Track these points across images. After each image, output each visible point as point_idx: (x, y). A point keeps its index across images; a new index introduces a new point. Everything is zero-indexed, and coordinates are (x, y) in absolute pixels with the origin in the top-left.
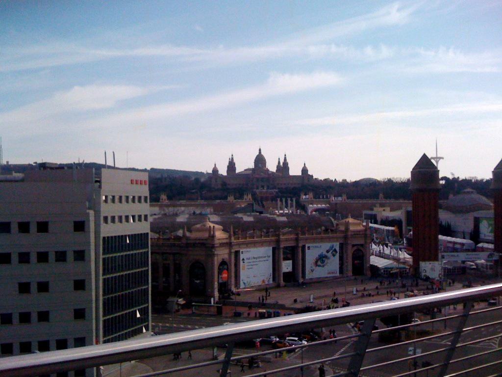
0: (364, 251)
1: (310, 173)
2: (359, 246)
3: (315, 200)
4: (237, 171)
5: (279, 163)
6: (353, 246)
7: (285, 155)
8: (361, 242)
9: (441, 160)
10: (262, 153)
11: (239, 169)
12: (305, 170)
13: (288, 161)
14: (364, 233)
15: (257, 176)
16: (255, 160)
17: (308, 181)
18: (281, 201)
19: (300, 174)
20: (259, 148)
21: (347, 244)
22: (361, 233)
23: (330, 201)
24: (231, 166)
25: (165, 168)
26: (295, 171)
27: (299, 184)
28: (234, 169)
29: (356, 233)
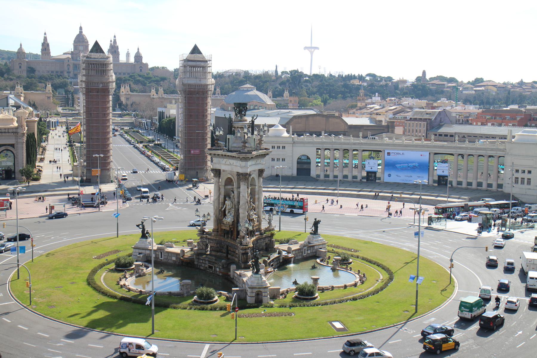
0: (15, 152)
1: (144, 61)
2: (6, 147)
4: (52, 54)
5: (111, 44)
7: (115, 37)
8: (12, 142)
9: (316, 50)
10: (84, 33)
11: (56, 51)
12: (138, 57)
13: (118, 44)
14: (14, 131)
16: (74, 41)
17: (141, 70)
19: (132, 60)
20: (80, 26)
22: (10, 131)
23: (150, 95)
24: (45, 47)
27: (128, 74)
28: (49, 53)
29: (4, 131)
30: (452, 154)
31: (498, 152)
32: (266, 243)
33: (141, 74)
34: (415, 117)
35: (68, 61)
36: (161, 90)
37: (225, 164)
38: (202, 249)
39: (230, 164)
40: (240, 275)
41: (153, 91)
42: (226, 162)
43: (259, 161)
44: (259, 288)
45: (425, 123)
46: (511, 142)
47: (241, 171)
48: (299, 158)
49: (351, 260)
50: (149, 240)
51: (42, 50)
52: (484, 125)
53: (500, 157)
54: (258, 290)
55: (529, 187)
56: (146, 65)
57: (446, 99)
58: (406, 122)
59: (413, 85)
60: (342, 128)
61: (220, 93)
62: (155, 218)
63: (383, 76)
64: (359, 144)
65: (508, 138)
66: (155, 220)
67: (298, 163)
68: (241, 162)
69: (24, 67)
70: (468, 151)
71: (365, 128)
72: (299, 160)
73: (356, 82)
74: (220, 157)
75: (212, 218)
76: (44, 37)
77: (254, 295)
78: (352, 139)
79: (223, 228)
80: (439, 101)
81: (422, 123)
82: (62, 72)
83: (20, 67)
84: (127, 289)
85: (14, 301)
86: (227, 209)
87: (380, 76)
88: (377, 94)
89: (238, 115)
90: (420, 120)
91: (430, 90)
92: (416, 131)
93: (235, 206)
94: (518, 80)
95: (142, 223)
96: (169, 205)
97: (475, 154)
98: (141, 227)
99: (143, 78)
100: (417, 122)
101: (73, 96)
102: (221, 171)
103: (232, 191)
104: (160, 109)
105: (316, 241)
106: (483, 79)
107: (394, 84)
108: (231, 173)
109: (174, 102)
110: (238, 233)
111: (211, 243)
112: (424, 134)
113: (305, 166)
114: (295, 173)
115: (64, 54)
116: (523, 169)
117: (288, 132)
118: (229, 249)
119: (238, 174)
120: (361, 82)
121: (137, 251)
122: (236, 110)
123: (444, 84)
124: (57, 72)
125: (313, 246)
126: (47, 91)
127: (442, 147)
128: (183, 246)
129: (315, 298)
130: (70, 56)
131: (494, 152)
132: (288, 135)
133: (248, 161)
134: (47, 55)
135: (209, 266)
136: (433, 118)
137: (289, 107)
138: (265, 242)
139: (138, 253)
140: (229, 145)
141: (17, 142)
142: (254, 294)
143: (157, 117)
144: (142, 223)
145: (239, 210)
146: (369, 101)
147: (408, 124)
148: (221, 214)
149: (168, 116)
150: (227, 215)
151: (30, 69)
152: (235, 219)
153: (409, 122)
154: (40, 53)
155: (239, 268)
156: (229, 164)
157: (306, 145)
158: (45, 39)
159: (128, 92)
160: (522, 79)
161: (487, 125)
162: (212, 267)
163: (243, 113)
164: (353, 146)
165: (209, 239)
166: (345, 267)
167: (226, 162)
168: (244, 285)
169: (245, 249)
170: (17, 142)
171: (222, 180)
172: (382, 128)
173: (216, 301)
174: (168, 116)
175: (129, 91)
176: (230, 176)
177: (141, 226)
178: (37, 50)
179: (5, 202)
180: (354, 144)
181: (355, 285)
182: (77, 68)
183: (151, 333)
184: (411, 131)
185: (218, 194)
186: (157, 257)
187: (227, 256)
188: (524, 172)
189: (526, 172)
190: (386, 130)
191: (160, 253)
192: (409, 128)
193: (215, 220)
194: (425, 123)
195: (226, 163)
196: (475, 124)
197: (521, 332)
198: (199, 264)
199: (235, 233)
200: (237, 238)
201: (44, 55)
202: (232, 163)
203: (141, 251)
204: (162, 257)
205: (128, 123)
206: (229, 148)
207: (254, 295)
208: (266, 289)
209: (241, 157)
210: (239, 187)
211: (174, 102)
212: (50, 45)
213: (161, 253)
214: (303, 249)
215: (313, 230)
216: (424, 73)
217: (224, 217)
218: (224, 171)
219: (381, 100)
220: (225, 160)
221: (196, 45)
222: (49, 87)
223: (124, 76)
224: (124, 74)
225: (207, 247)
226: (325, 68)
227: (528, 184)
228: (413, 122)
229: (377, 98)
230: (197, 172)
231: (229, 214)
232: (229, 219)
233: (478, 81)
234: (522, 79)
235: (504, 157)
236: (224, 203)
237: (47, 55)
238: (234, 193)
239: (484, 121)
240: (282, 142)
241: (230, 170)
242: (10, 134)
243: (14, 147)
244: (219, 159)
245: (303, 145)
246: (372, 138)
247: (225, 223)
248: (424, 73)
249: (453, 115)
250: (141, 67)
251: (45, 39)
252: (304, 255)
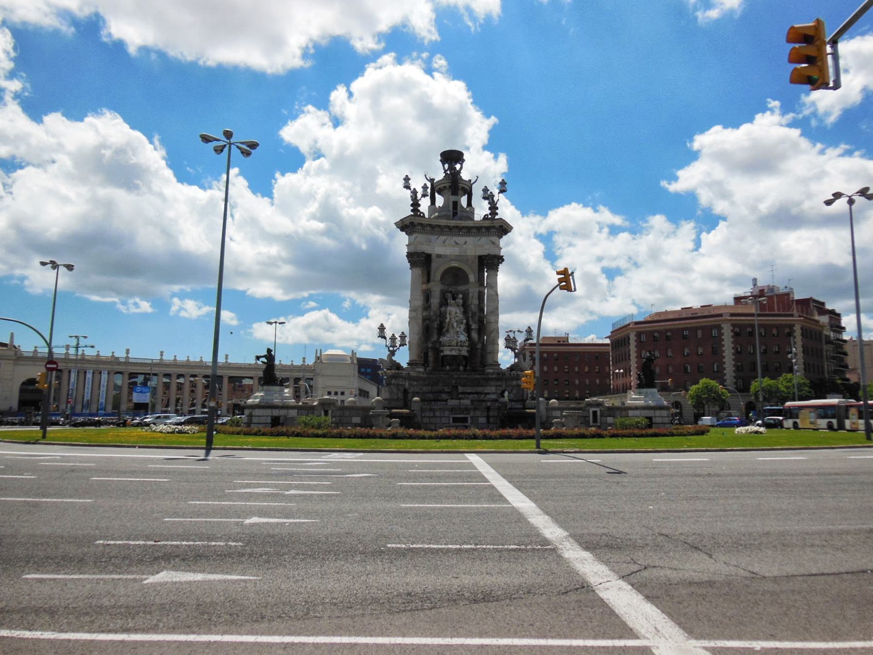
39: (456, 243)
42: (444, 242)
48: (24, 384)
102: (434, 257)
116: (336, 390)
139: (269, 420)
156: (454, 243)
162: (467, 418)
164: (116, 367)
167: (444, 242)
176: (455, 264)
195: (447, 242)
203: (276, 413)
241: (458, 254)
245: (32, 363)
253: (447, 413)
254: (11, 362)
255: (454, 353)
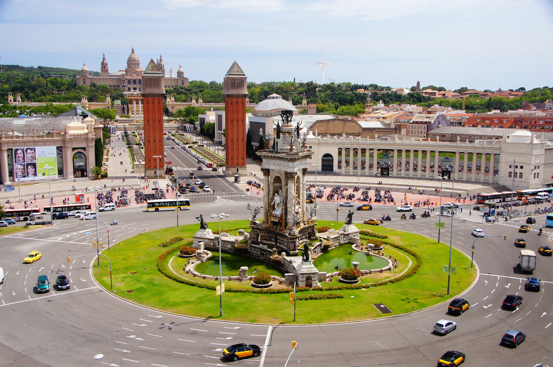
0: (86, 154)
1: (185, 76)
3: (176, 103)
4: (110, 72)
5: (157, 62)
6: (74, 149)
7: (161, 56)
12: (180, 74)
14: (85, 136)
15: (129, 78)
16: (128, 61)
17: (183, 84)
18: (137, 103)
19: (175, 76)
21: (65, 147)
23: (191, 105)
24: (104, 66)
25: (55, 67)
26: (170, 73)
27: (173, 87)
30: (454, 153)
31: (494, 151)
32: (309, 233)
33: (183, 86)
34: (417, 120)
35: (123, 77)
36: (201, 101)
37: (274, 165)
38: (254, 238)
40: (291, 262)
41: (194, 101)
42: (274, 163)
43: (303, 161)
44: (309, 274)
45: (426, 126)
46: (505, 142)
47: (290, 170)
49: (382, 247)
50: (207, 230)
51: (102, 68)
52: (475, 127)
53: (496, 154)
54: (308, 275)
55: (521, 180)
56: (186, 79)
57: (438, 105)
58: (409, 125)
59: (409, 94)
60: (357, 130)
61: (248, 102)
62: (222, 216)
63: (383, 86)
64: (374, 144)
65: (504, 137)
66: (222, 217)
67: (323, 160)
68: (288, 163)
69: (88, 83)
70: (468, 149)
71: (376, 130)
72: (324, 158)
73: (362, 91)
74: (269, 159)
75: (262, 211)
76: (103, 57)
77: (305, 280)
78: (368, 140)
79: (272, 220)
80: (432, 107)
81: (423, 125)
82: (118, 86)
83: (84, 83)
84: (193, 274)
85: (97, 286)
86: (276, 203)
87: (381, 86)
88: (381, 101)
89: (285, 121)
90: (422, 123)
91: (423, 97)
92: (418, 133)
93: (283, 201)
94: (497, 89)
95: (201, 216)
96: (217, 198)
97: (474, 152)
98: (200, 219)
99: (184, 90)
100: (419, 125)
101: (128, 106)
102: (270, 170)
103: (280, 188)
104: (200, 116)
105: (350, 229)
106: (467, 88)
107: (394, 93)
108: (279, 172)
109: (212, 109)
110: (286, 224)
111: (261, 232)
112: (425, 135)
113: (329, 163)
114: (320, 169)
115: (120, 71)
117: (314, 134)
118: (278, 238)
119: (286, 173)
120: (365, 91)
121: (197, 240)
122: (283, 116)
123: (435, 93)
124: (114, 86)
125: (348, 234)
126: (107, 102)
127: (446, 146)
128: (235, 235)
129: (357, 282)
130: (124, 73)
131: (491, 151)
132: (314, 137)
133: (295, 162)
134: (106, 72)
135: (261, 253)
136: (433, 121)
137: (308, 113)
138: (308, 232)
139: (198, 242)
140: (277, 148)
141: (88, 146)
142: (305, 278)
143: (198, 123)
144: (201, 216)
145: (286, 204)
146: (375, 107)
147: (411, 127)
148: (271, 207)
149: (208, 122)
150: (276, 209)
151: (91, 84)
152: (284, 212)
153: (412, 125)
154: (100, 71)
155: (288, 255)
156: (277, 164)
157: (329, 145)
158: (104, 59)
159: (173, 101)
160: (500, 88)
161: (477, 127)
163: (289, 119)
164: (369, 146)
165: (259, 229)
166: (377, 252)
167: (274, 163)
168: (294, 270)
169: (294, 239)
170: (88, 146)
171: (271, 178)
172: (391, 130)
173: (271, 285)
174: (208, 122)
175: (174, 101)
176: (278, 175)
177: (200, 219)
178: (98, 69)
179: (81, 197)
180: (371, 144)
181: (390, 269)
182: (130, 82)
183: (220, 315)
184: (414, 132)
185: (267, 191)
186: (215, 244)
187: (276, 244)
188: (517, 167)
189: (519, 167)
190: (394, 132)
191: (217, 242)
192: (412, 130)
193: (265, 213)
194: (426, 126)
195: (275, 163)
196: (467, 126)
197: (545, 313)
198: (252, 251)
199: (284, 224)
200: (286, 228)
201: (104, 72)
202: (280, 164)
203: (200, 240)
204: (218, 245)
205: (175, 127)
206: (277, 150)
207: (304, 279)
208: (315, 275)
209: (289, 158)
210: (287, 184)
211: (212, 109)
212: (108, 64)
213: (218, 242)
214: (340, 237)
215: (348, 220)
216: (418, 83)
217: (273, 210)
218: (272, 170)
219: (384, 106)
220: (274, 161)
221: (235, 61)
222: (109, 99)
223: (169, 88)
224: (169, 87)
225: (258, 236)
226: (334, 80)
227: (520, 177)
228: (415, 125)
229: (381, 105)
230: (238, 169)
231: (278, 208)
232: (278, 212)
233: (462, 91)
234: (500, 88)
235: (499, 154)
236: (273, 199)
237: (106, 72)
238: (281, 189)
239: (475, 124)
240: (309, 142)
242: (82, 139)
243: (85, 150)
244: (269, 160)
246: (385, 139)
247: (274, 215)
248: (418, 83)
249: (448, 119)
250: (183, 81)
251: (104, 59)
252: (341, 242)
253: (259, 250)
254: (317, 145)
255: (274, 220)
